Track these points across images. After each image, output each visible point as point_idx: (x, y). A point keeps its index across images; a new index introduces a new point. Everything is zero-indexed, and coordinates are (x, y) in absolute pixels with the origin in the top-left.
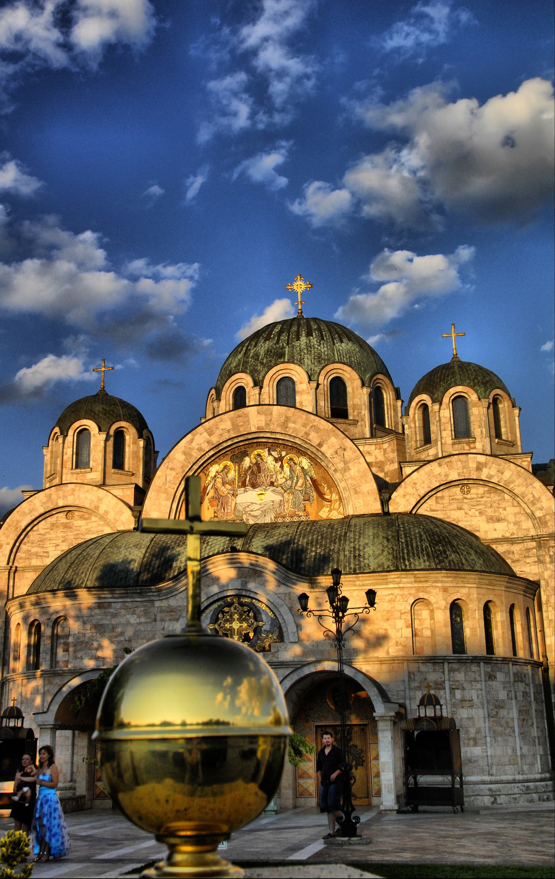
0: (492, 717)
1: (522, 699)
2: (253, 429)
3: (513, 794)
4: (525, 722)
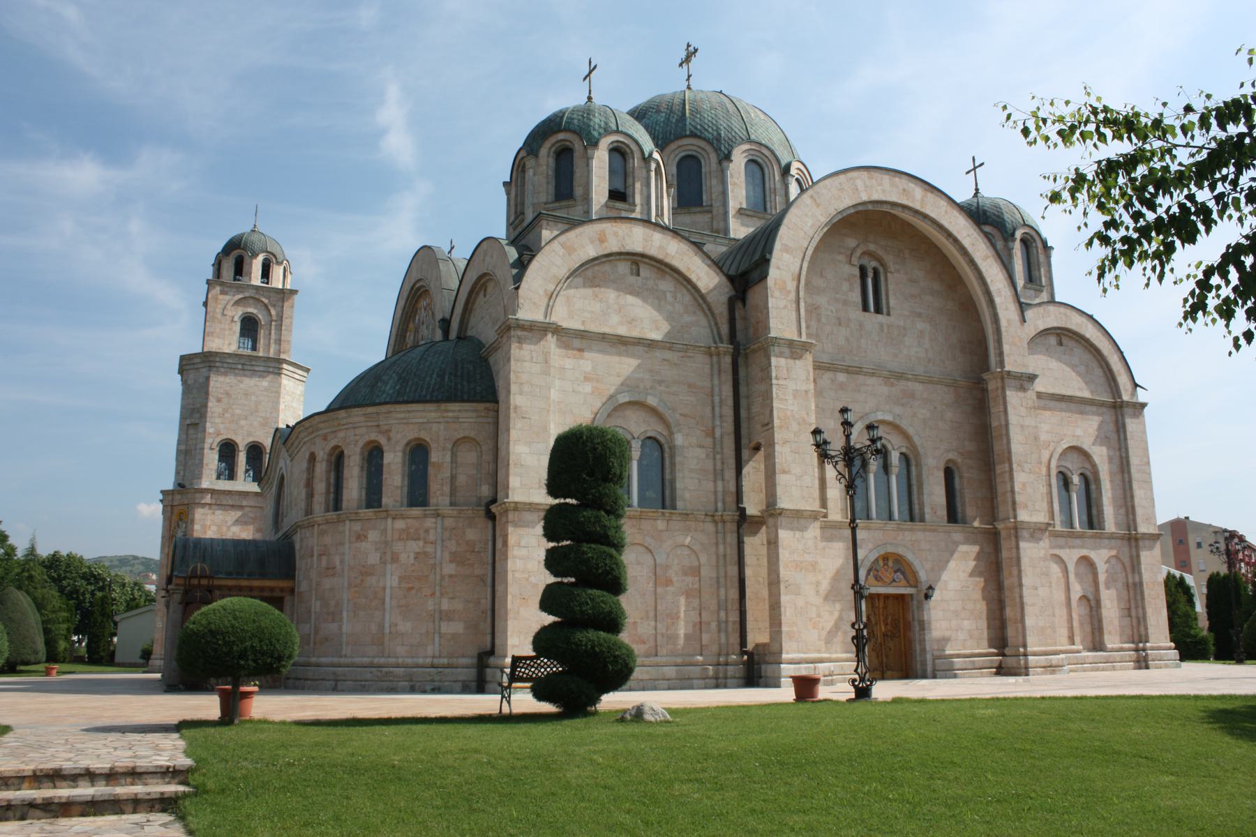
0: (356, 586)
1: (412, 561)
2: (413, 281)
3: (366, 681)
4: (414, 592)
